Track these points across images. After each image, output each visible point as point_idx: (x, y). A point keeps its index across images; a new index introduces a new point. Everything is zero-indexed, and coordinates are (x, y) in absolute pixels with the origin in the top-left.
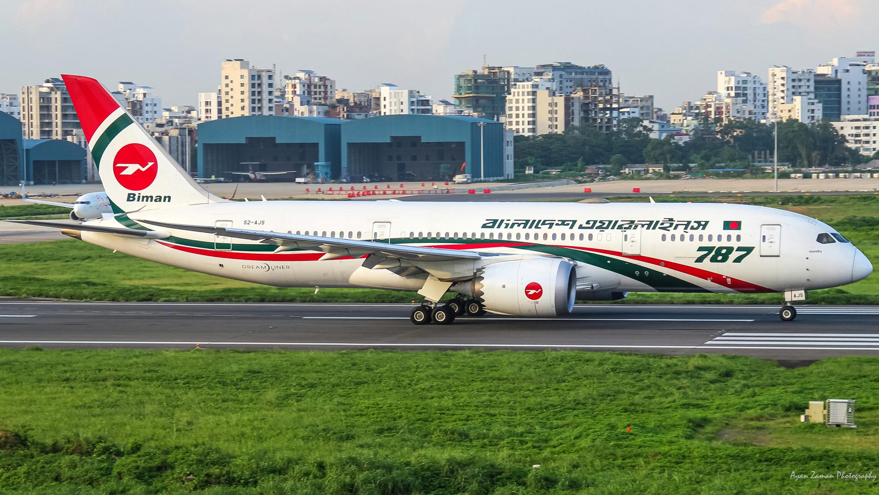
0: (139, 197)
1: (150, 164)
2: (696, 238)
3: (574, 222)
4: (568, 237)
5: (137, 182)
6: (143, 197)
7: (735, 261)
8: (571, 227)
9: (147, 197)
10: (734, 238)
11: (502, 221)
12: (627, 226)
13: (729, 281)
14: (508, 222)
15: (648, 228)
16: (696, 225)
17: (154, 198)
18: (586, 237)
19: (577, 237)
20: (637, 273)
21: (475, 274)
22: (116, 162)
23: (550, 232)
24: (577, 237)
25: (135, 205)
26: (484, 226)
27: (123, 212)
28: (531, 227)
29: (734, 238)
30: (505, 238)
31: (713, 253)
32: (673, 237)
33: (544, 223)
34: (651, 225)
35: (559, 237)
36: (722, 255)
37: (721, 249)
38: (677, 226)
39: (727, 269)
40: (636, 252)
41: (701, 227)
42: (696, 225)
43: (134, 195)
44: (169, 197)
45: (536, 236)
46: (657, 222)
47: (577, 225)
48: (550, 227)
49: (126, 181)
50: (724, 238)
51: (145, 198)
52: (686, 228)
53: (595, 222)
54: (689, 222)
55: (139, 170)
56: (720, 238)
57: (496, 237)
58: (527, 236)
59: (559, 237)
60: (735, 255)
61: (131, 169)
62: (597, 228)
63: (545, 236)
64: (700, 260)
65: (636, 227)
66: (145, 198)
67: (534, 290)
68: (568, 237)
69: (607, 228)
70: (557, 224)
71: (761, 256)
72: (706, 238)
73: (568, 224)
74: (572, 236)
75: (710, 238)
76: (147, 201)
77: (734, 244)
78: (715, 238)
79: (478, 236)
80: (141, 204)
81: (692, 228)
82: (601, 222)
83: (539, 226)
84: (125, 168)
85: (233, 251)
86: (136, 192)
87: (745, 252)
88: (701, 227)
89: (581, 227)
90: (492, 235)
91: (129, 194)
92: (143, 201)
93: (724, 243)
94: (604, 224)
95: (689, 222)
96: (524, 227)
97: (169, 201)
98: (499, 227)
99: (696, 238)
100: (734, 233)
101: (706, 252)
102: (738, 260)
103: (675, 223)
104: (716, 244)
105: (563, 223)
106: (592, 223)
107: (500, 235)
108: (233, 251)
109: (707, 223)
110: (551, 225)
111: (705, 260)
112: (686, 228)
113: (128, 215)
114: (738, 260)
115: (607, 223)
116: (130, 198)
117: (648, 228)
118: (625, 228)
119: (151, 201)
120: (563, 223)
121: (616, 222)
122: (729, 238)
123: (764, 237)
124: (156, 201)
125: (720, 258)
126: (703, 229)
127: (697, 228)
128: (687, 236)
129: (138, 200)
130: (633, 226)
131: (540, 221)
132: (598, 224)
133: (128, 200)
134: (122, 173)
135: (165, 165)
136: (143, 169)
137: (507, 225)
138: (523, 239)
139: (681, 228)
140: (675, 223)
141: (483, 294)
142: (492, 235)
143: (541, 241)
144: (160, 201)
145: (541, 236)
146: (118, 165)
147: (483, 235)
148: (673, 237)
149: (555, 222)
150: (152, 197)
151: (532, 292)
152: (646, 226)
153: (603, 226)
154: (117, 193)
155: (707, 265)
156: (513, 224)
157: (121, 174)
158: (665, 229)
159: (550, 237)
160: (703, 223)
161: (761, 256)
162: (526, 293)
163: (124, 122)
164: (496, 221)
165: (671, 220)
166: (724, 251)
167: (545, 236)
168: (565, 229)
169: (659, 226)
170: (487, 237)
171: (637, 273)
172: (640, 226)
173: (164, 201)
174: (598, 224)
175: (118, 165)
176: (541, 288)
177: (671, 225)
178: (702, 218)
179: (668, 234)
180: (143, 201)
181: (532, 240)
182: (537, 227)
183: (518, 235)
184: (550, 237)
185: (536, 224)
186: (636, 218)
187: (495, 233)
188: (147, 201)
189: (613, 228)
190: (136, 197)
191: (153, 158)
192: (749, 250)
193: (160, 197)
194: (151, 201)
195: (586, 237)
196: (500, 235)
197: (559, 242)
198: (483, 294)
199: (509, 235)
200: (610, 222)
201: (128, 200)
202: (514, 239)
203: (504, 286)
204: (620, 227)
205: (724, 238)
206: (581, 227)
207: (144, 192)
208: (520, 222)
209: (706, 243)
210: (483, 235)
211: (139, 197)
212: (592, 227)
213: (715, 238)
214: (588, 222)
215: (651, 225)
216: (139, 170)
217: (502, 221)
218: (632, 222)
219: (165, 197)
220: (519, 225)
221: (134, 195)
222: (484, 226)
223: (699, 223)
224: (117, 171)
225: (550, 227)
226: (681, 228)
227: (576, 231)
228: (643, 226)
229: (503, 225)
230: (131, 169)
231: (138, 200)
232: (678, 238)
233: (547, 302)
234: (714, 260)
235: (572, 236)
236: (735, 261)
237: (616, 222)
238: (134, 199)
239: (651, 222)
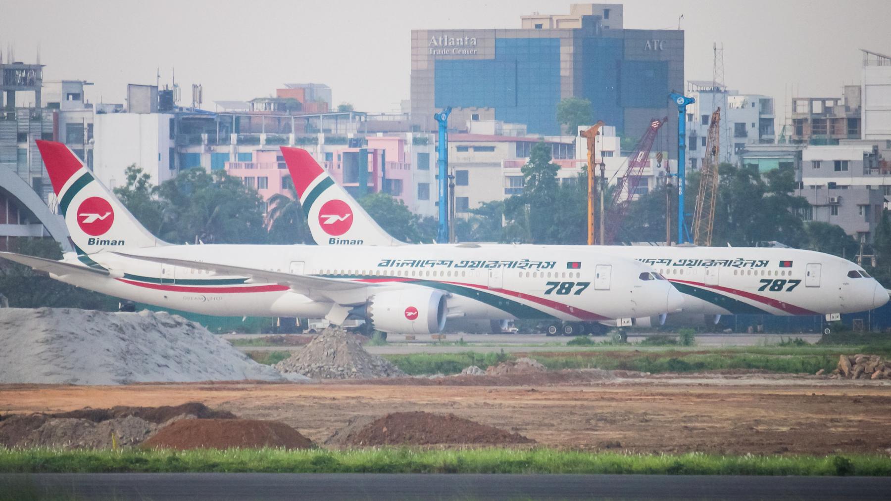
0: (98, 241)
1: (108, 214)
2: (546, 274)
4: (446, 274)
5: (96, 229)
6: (102, 241)
7: (576, 294)
9: (105, 242)
10: (575, 275)
11: (394, 261)
12: (493, 265)
13: (571, 309)
14: (399, 262)
15: (509, 267)
18: (460, 274)
19: (453, 274)
20: (500, 303)
21: (367, 300)
22: (80, 211)
23: (432, 270)
24: (453, 274)
25: (95, 248)
26: (380, 265)
27: (85, 253)
28: (417, 265)
29: (575, 275)
30: (396, 275)
31: (559, 287)
32: (528, 275)
33: (427, 263)
34: (512, 265)
35: (438, 274)
36: (565, 288)
37: (564, 284)
39: (569, 300)
40: (499, 286)
41: (550, 266)
42: (546, 265)
43: (94, 239)
44: (123, 242)
45: (421, 273)
46: (516, 263)
47: (453, 264)
48: (432, 266)
49: (87, 228)
50: (567, 275)
51: (103, 243)
54: (541, 263)
55: (98, 219)
56: (564, 275)
57: (389, 274)
58: (413, 273)
59: (438, 274)
60: (575, 288)
61: (92, 218)
62: (469, 267)
63: (428, 273)
64: (548, 292)
65: (499, 266)
66: (103, 243)
67: (412, 313)
68: (446, 274)
69: (477, 266)
70: (438, 264)
71: (596, 290)
72: (553, 274)
73: (446, 264)
74: (449, 274)
75: (556, 275)
76: (105, 244)
77: (575, 280)
78: (560, 275)
79: (374, 273)
80: (99, 247)
81: (543, 267)
82: (472, 262)
83: (424, 265)
84: (86, 217)
85: (176, 285)
86: (96, 237)
87: (583, 287)
88: (550, 266)
90: (385, 272)
91: (90, 239)
92: (101, 244)
93: (568, 279)
94: (475, 263)
96: (412, 266)
97: (123, 244)
98: (392, 265)
99: (546, 274)
100: (574, 271)
101: (553, 286)
102: (578, 292)
104: (561, 280)
106: (465, 263)
107: (392, 272)
108: (176, 285)
109: (554, 263)
110: (433, 264)
111: (552, 293)
113: (89, 256)
114: (578, 292)
115: (477, 263)
116: (91, 242)
117: (509, 267)
118: (491, 267)
119: (108, 244)
121: (484, 262)
122: (571, 275)
123: (598, 275)
124: (112, 244)
125: (564, 291)
126: (552, 267)
127: (547, 267)
128: (539, 273)
129: (97, 244)
130: (497, 265)
131: (424, 261)
132: (470, 264)
134: (85, 222)
135: (121, 215)
136: (102, 218)
137: (398, 264)
138: (410, 276)
139: (534, 267)
141: (372, 315)
142: (385, 272)
143: (424, 277)
144: (116, 244)
145: (424, 273)
146: (81, 215)
147: (378, 272)
148: (528, 275)
149: (438, 262)
151: (410, 314)
152: (507, 266)
153: (473, 265)
154: (81, 238)
155: (554, 297)
156: (403, 264)
157: (85, 222)
158: (522, 267)
159: (431, 274)
160: (551, 263)
161: (596, 290)
162: (406, 315)
163: (87, 179)
164: (389, 261)
165: (527, 260)
166: (567, 286)
167: (428, 273)
168: (444, 268)
170: (382, 274)
171: (500, 303)
172: (502, 266)
173: (119, 244)
175: (81, 215)
176: (417, 311)
177: (527, 265)
178: (551, 261)
179: (524, 271)
180: (101, 244)
181: (417, 277)
182: (422, 266)
183: (406, 273)
184: (431, 274)
185: (421, 263)
186: (500, 260)
187: (389, 271)
188: (105, 244)
189: (481, 267)
190: (96, 242)
191: (110, 209)
192: (586, 285)
193: (116, 242)
194: (108, 244)
195: (460, 274)
196: (392, 272)
197: (438, 278)
198: (372, 315)
199: (399, 272)
200: (479, 262)
201: (89, 243)
202: (403, 275)
203: (389, 309)
204: (487, 266)
205: (567, 275)
206: (456, 266)
207: (102, 237)
208: (408, 262)
209: (553, 279)
210: (378, 272)
211: (98, 241)
213: (560, 275)
214: (462, 262)
215: (512, 265)
216: (98, 219)
217: (394, 261)
218: (497, 262)
219: (120, 242)
220: (408, 264)
221: (94, 239)
222: (380, 265)
224: (80, 220)
225: (432, 266)
226: (534, 267)
227: (452, 268)
228: (505, 265)
229: (395, 264)
230: (92, 218)
231: (97, 244)
232: (531, 275)
233: (422, 321)
234: (559, 292)
235: (449, 274)
236: (576, 294)
237: (484, 262)
238: (94, 243)
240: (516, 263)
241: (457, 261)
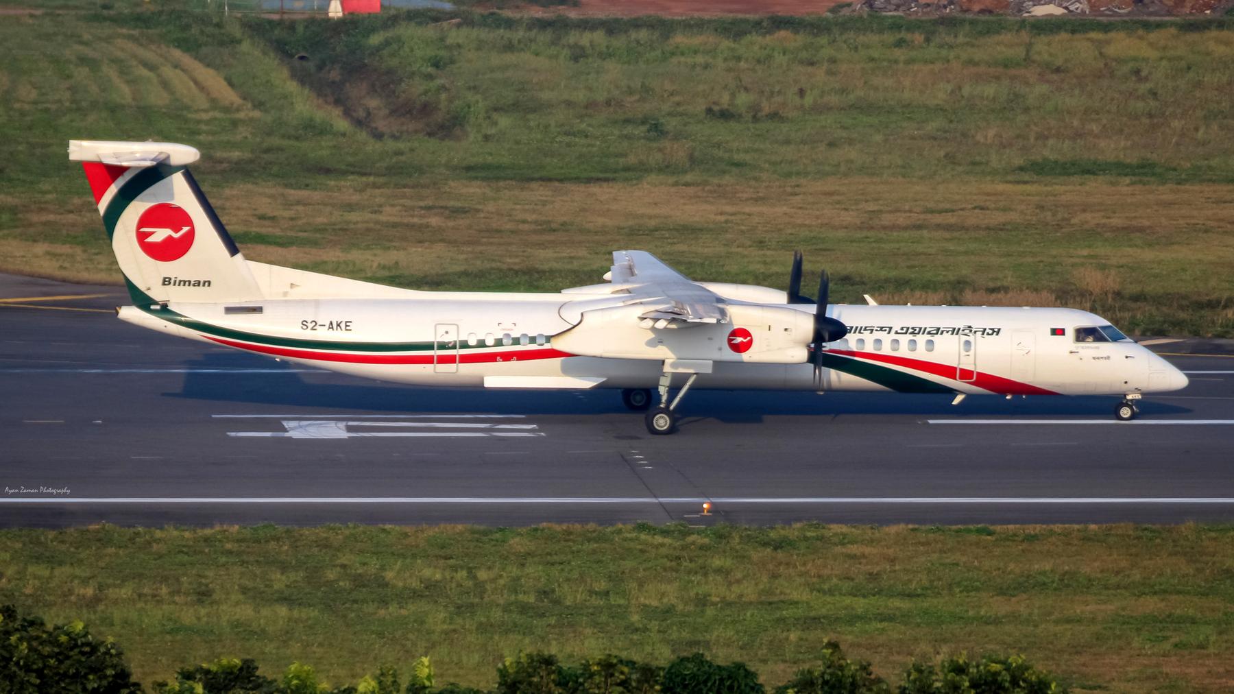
0: (175, 281)
3: (891, 328)
6: (180, 281)
8: (889, 333)
9: (185, 282)
16: (990, 332)
17: (192, 283)
33: (865, 330)
38: (975, 332)
42: (990, 332)
46: (959, 329)
47: (893, 331)
48: (871, 333)
51: (182, 283)
52: (983, 334)
53: (908, 328)
54: (985, 329)
62: (911, 333)
66: (182, 283)
69: (919, 333)
76: (184, 285)
81: (988, 334)
82: (912, 328)
89: (897, 333)
92: (179, 285)
95: (985, 329)
103: (974, 330)
105: (882, 329)
106: (905, 329)
109: (999, 330)
110: (872, 331)
112: (983, 334)
115: (918, 329)
119: (189, 285)
120: (882, 329)
121: (925, 329)
124: (194, 285)
126: (997, 335)
127: (992, 334)
129: (175, 284)
131: (861, 328)
132: (910, 330)
133: (164, 284)
140: (974, 330)
150: (190, 282)
157: (150, 239)
165: (970, 327)
169: (960, 331)
174: (910, 330)
178: (996, 326)
182: (860, 332)
186: (942, 326)
188: (184, 285)
190: (172, 282)
204: (929, 333)
206: (897, 333)
211: (175, 281)
212: (906, 333)
214: (902, 329)
223: (993, 329)
225: (871, 333)
228: (947, 332)
231: (175, 284)
237: (925, 329)
239: (954, 329)
240: (959, 329)
241: (897, 328)
